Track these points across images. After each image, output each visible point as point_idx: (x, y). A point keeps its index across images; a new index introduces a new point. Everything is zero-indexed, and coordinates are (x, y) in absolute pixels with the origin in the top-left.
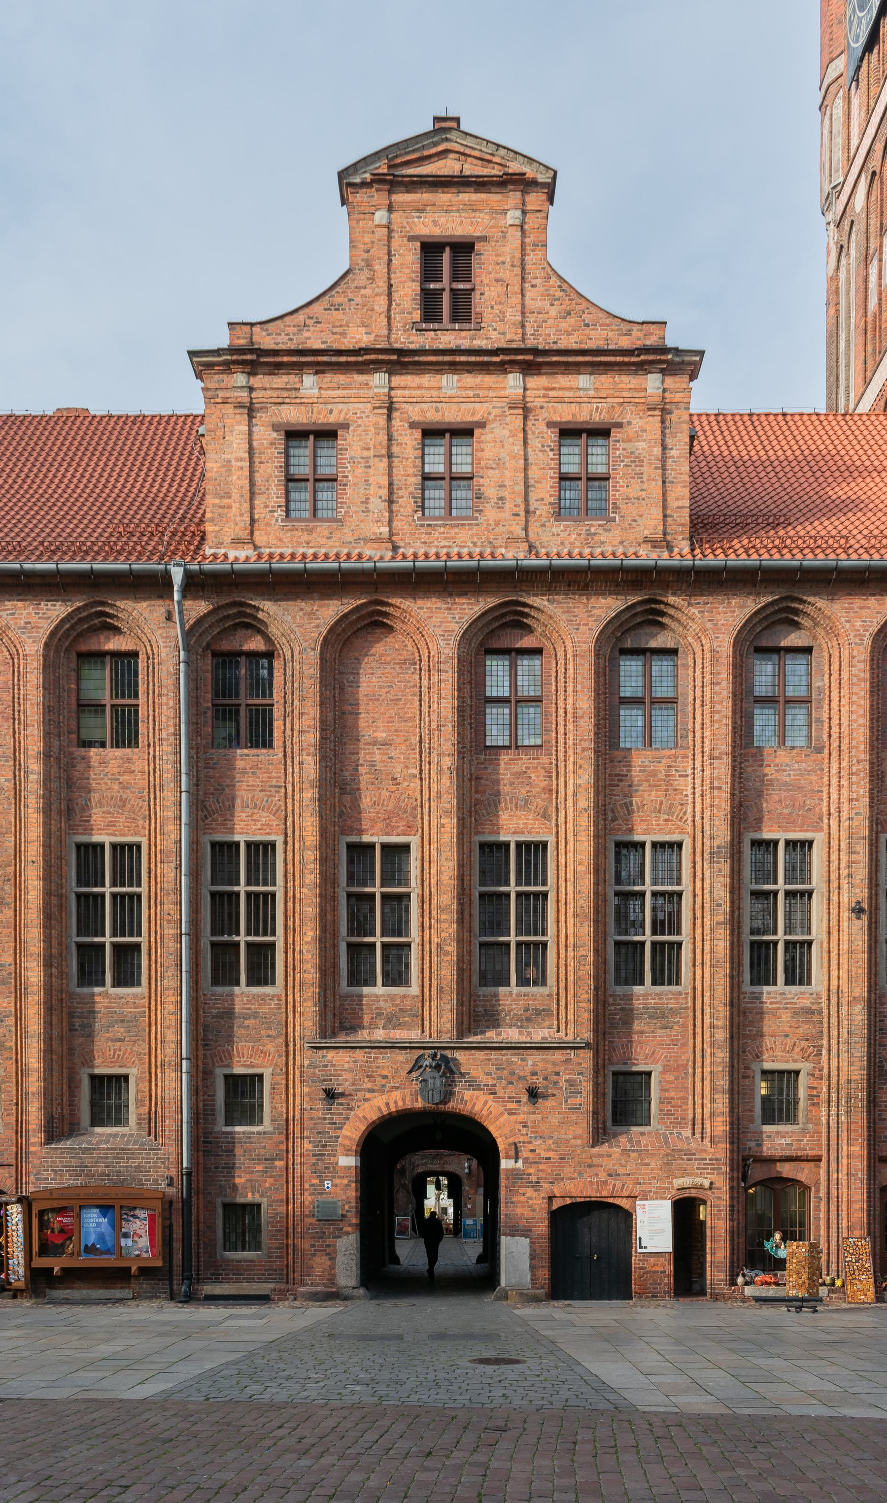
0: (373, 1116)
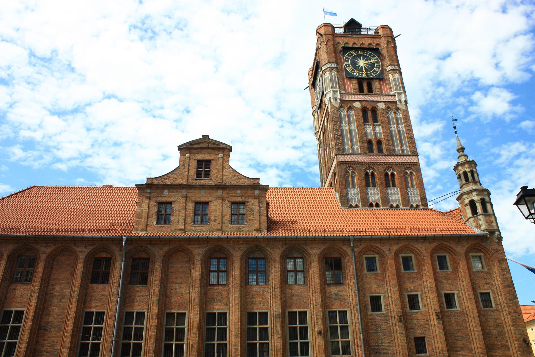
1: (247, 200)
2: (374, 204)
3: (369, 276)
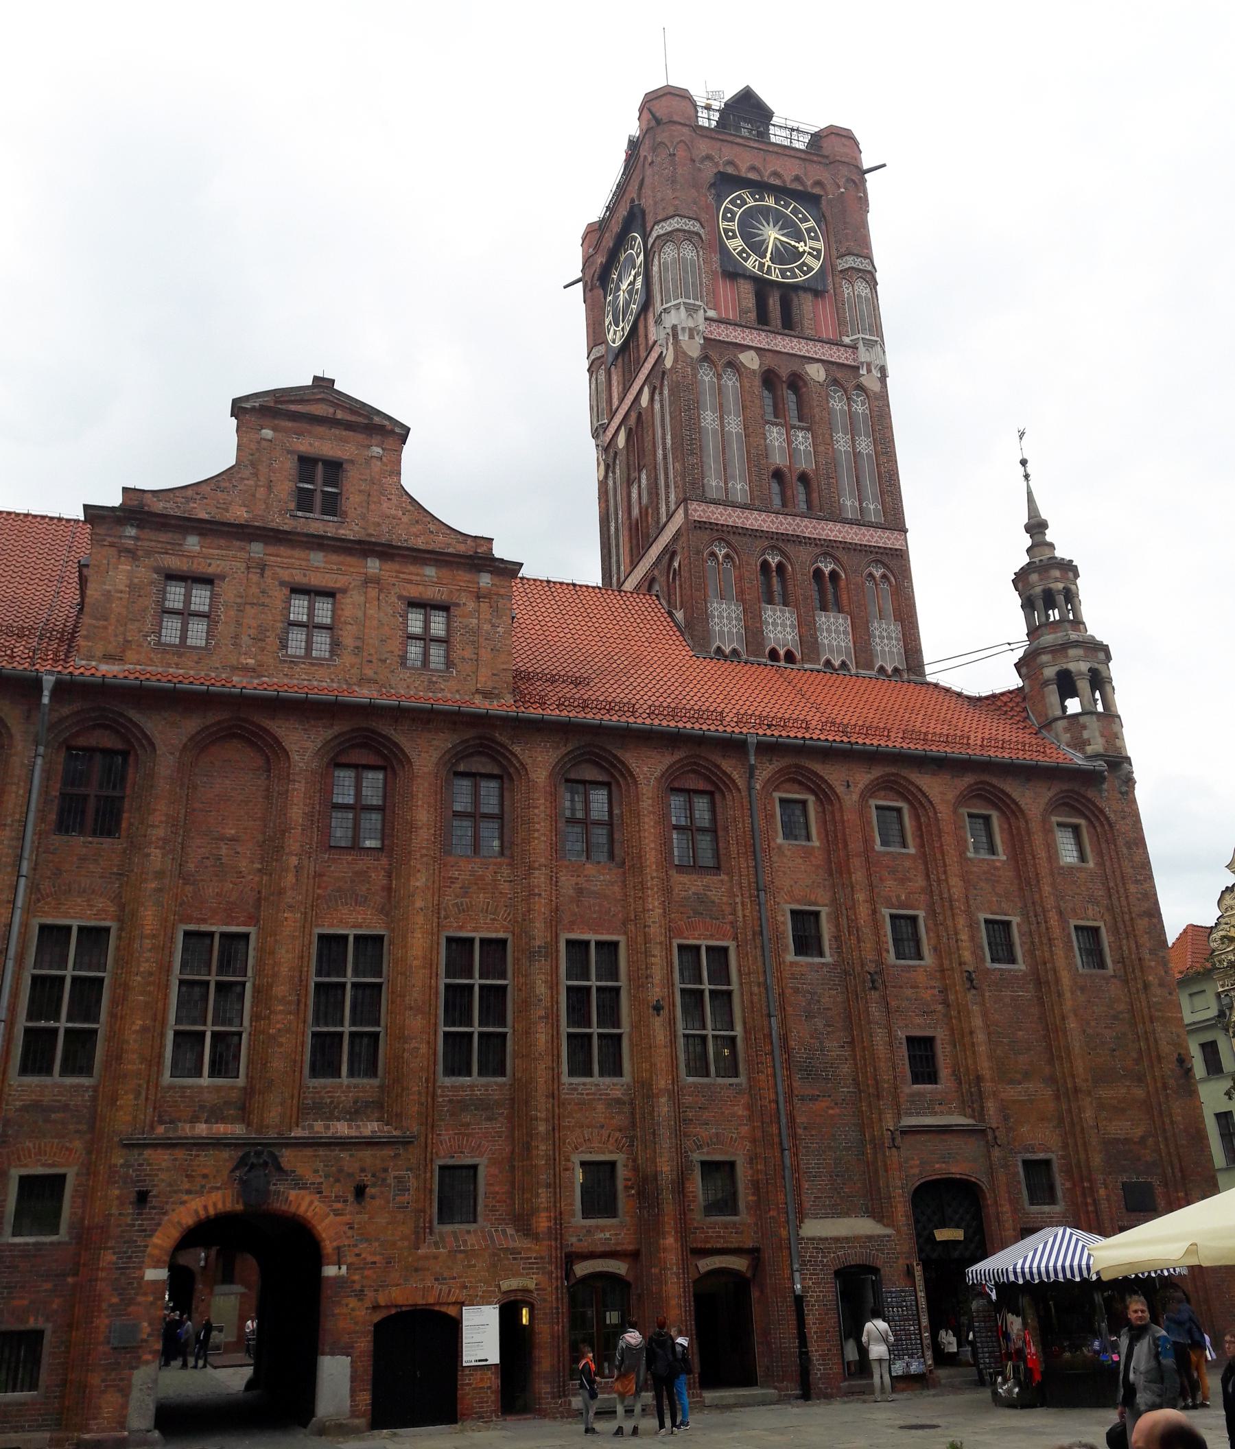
0: (189, 1221)
1: (455, 600)
2: (782, 653)
3: (788, 853)
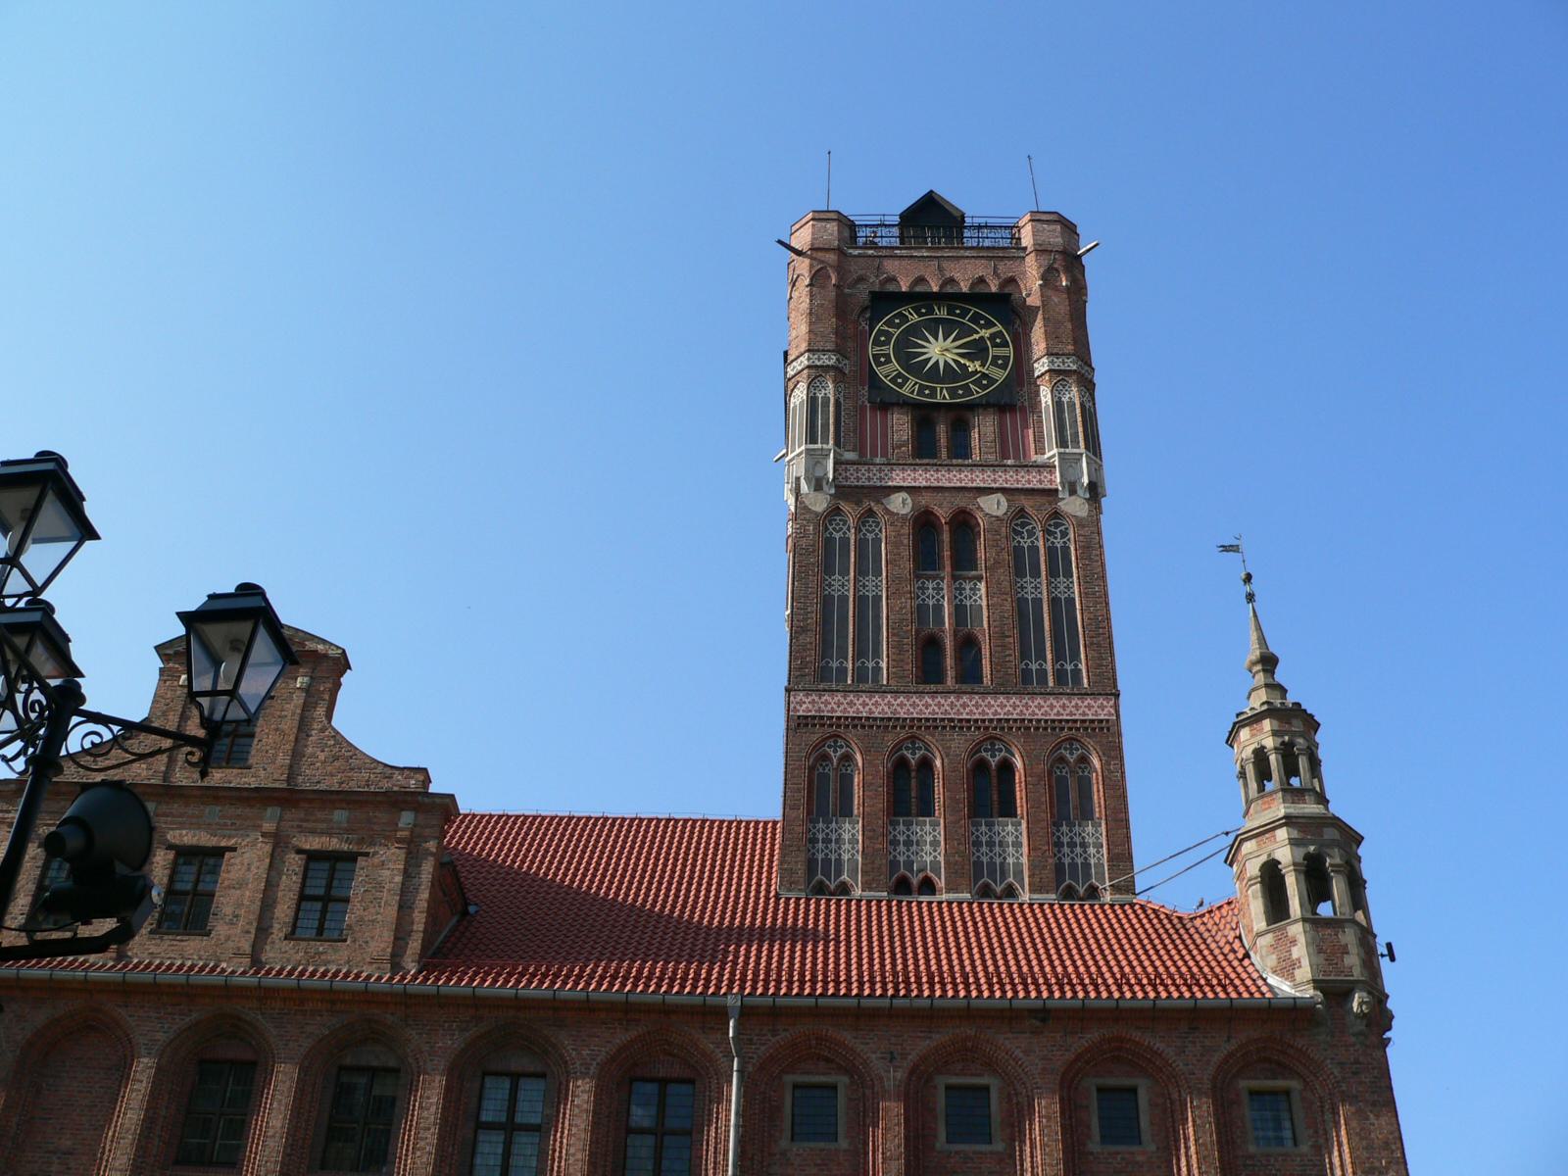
2: (915, 881)
